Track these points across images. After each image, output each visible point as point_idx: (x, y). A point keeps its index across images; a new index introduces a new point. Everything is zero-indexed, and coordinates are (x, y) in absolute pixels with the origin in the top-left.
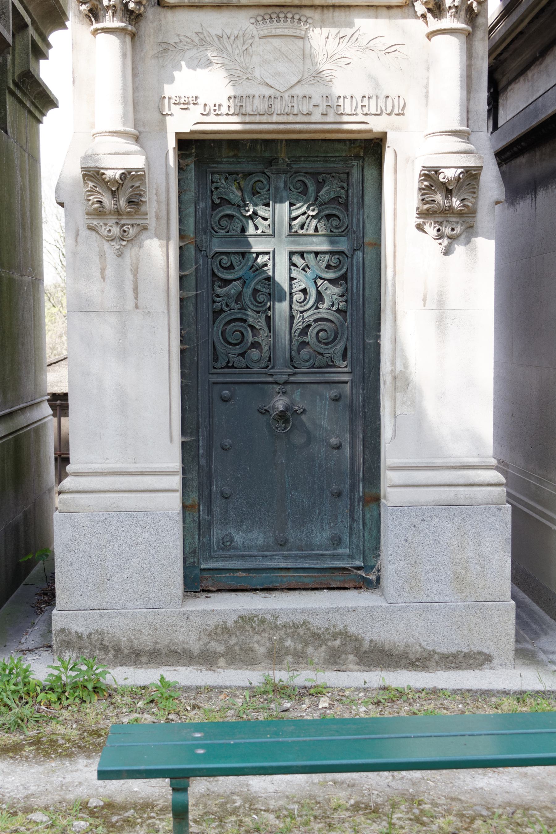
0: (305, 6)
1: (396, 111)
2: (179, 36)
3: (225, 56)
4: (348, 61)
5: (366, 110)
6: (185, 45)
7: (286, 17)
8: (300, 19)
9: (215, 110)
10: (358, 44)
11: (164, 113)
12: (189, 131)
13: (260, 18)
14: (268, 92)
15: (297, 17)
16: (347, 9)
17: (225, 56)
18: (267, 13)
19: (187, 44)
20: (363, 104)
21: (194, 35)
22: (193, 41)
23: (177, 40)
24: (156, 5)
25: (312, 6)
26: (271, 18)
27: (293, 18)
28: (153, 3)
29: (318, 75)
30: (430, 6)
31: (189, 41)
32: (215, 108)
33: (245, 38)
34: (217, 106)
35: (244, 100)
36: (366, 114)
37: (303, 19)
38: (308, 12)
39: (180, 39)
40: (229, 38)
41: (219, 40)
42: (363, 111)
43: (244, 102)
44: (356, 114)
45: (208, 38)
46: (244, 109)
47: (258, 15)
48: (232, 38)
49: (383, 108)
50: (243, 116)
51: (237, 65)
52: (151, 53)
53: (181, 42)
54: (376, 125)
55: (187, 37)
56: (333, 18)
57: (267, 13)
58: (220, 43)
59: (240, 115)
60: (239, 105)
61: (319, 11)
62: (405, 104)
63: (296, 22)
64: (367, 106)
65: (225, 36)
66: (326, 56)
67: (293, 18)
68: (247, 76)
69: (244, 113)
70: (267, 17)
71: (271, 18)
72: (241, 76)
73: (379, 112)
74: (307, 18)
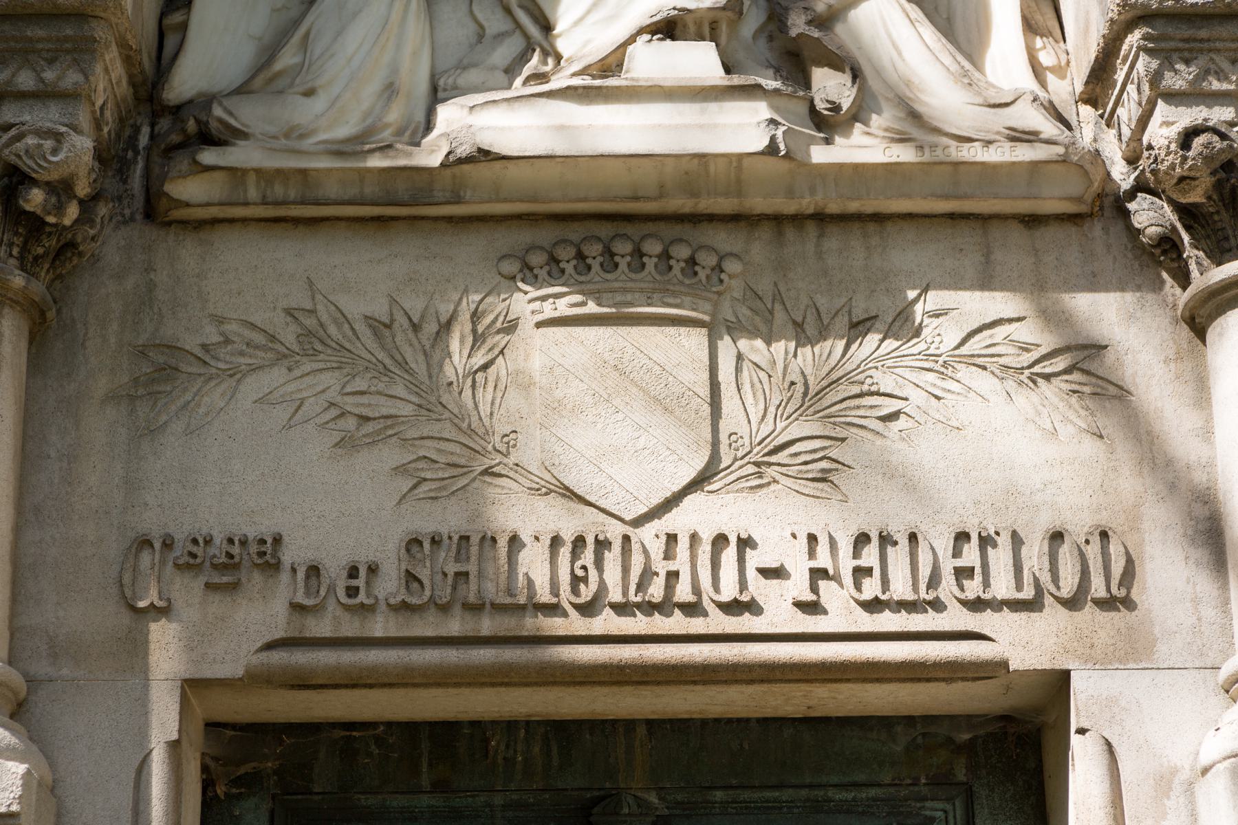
0: (711, 218)
1: (1098, 588)
2: (220, 320)
3: (400, 390)
4: (890, 406)
5: (973, 588)
6: (242, 354)
7: (638, 253)
8: (692, 262)
9: (352, 592)
10: (922, 346)
11: (142, 604)
12: (240, 672)
13: (537, 259)
14: (569, 523)
15: (682, 252)
16: (872, 227)
17: (400, 390)
18: (564, 241)
19: (251, 351)
20: (960, 563)
21: (280, 318)
22: (273, 338)
23: (216, 338)
24: (139, 217)
25: (735, 218)
26: (580, 256)
27: (666, 256)
28: (127, 212)
29: (773, 459)
30: (1195, 197)
31: (259, 338)
32: (354, 583)
33: (480, 329)
34: (363, 572)
35: (474, 550)
36: (977, 605)
37: (707, 260)
38: (722, 238)
39: (222, 334)
40: (416, 328)
41: (376, 333)
42: (962, 590)
43: (473, 559)
44: (937, 605)
45: (332, 330)
46: (473, 586)
47: (531, 248)
48: (431, 328)
49: (1045, 578)
50: (468, 616)
51: (448, 425)
52: (102, 385)
53: (227, 341)
54: (1023, 644)
55: (253, 326)
56: (820, 255)
57: (564, 241)
58: (383, 347)
59: (457, 609)
60: (452, 568)
61: (766, 231)
62: (1130, 562)
63: (676, 270)
64: (978, 570)
65: (401, 320)
66: (800, 388)
67: (666, 256)
68: (488, 463)
69: (472, 598)
70: (565, 253)
71: (580, 256)
72: (462, 461)
73: (1028, 593)
74: (721, 259)
